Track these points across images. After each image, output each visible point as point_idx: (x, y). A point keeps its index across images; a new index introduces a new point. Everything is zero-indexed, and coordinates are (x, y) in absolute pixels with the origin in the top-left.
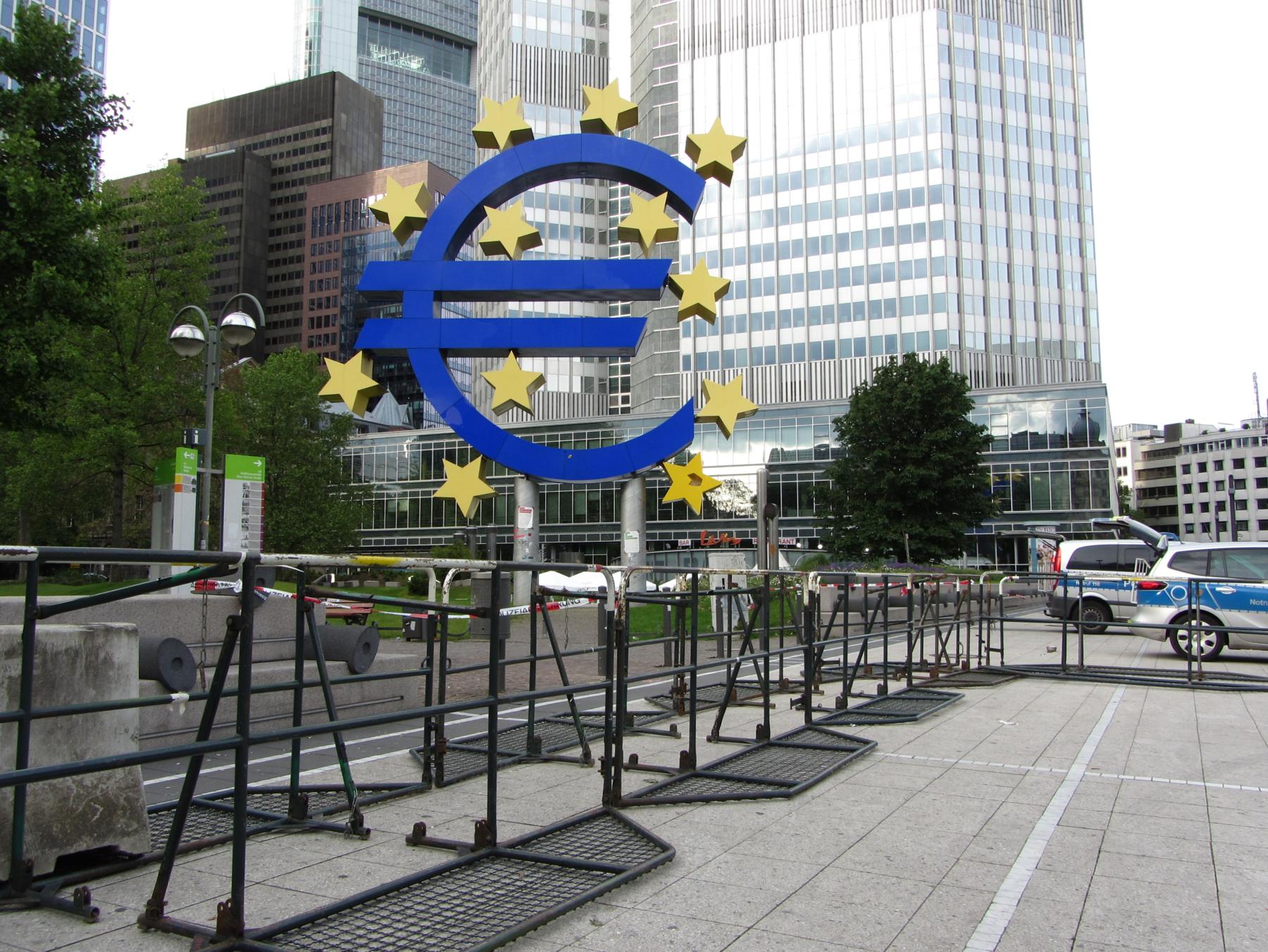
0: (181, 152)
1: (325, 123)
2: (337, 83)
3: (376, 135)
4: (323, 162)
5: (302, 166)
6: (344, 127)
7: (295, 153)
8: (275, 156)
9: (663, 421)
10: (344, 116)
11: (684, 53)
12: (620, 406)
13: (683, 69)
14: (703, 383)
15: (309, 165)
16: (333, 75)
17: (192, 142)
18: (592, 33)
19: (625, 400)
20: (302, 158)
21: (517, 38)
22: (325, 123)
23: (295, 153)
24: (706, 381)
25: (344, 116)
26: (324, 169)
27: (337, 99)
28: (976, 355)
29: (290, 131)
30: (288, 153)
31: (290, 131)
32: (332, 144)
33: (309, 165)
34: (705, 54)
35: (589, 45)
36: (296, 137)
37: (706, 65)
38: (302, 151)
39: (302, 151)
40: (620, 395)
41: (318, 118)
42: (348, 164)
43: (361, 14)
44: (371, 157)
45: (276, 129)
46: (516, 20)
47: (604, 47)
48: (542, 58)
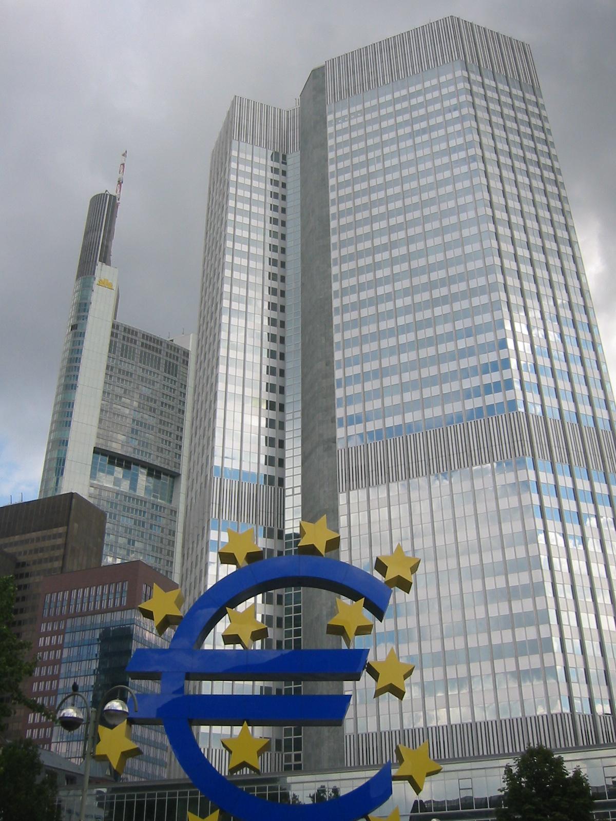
2: (74, 501)
3: (99, 540)
4: (57, 559)
5: (40, 561)
7: (36, 551)
8: (20, 553)
9: (367, 780)
10: (76, 525)
11: (342, 484)
12: (293, 762)
13: (342, 498)
14: (397, 747)
15: (46, 560)
16: (71, 495)
18: (272, 471)
19: (298, 757)
22: (61, 530)
23: (36, 551)
24: (401, 747)
25: (76, 525)
27: (73, 512)
28: (584, 716)
30: (31, 551)
32: (65, 545)
33: (46, 560)
34: (358, 487)
35: (270, 480)
36: (38, 539)
37: (358, 496)
38: (42, 550)
39: (42, 550)
40: (293, 753)
41: (57, 526)
45: (24, 533)
47: (281, 482)
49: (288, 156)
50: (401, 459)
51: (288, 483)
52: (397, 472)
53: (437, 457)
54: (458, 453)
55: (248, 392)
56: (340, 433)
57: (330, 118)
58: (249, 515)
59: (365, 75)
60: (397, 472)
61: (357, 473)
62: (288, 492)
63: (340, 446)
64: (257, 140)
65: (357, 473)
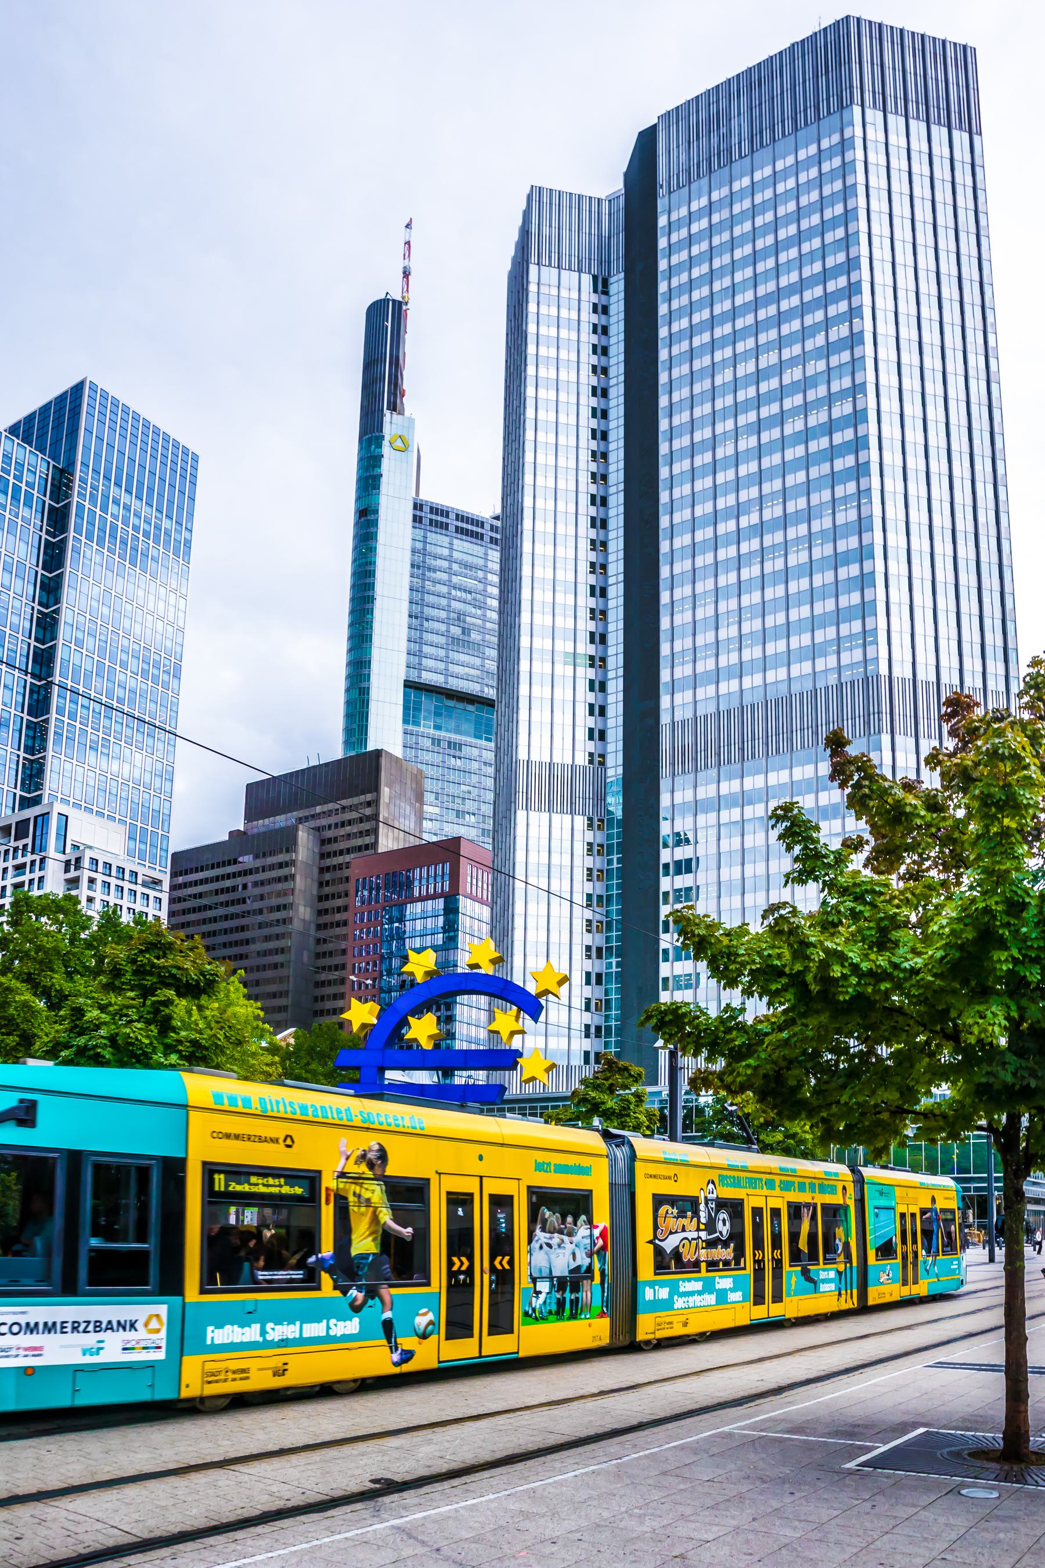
11: (665, 770)
13: (664, 784)
21: (522, 755)
48: (545, 773)
49: (612, 280)
50: (735, 736)
52: (729, 752)
53: (777, 735)
54: (802, 729)
55: (559, 645)
56: (665, 701)
57: (662, 221)
58: (562, 804)
59: (714, 140)
60: (729, 752)
61: (683, 754)
63: (665, 719)
64: (565, 263)
65: (683, 754)
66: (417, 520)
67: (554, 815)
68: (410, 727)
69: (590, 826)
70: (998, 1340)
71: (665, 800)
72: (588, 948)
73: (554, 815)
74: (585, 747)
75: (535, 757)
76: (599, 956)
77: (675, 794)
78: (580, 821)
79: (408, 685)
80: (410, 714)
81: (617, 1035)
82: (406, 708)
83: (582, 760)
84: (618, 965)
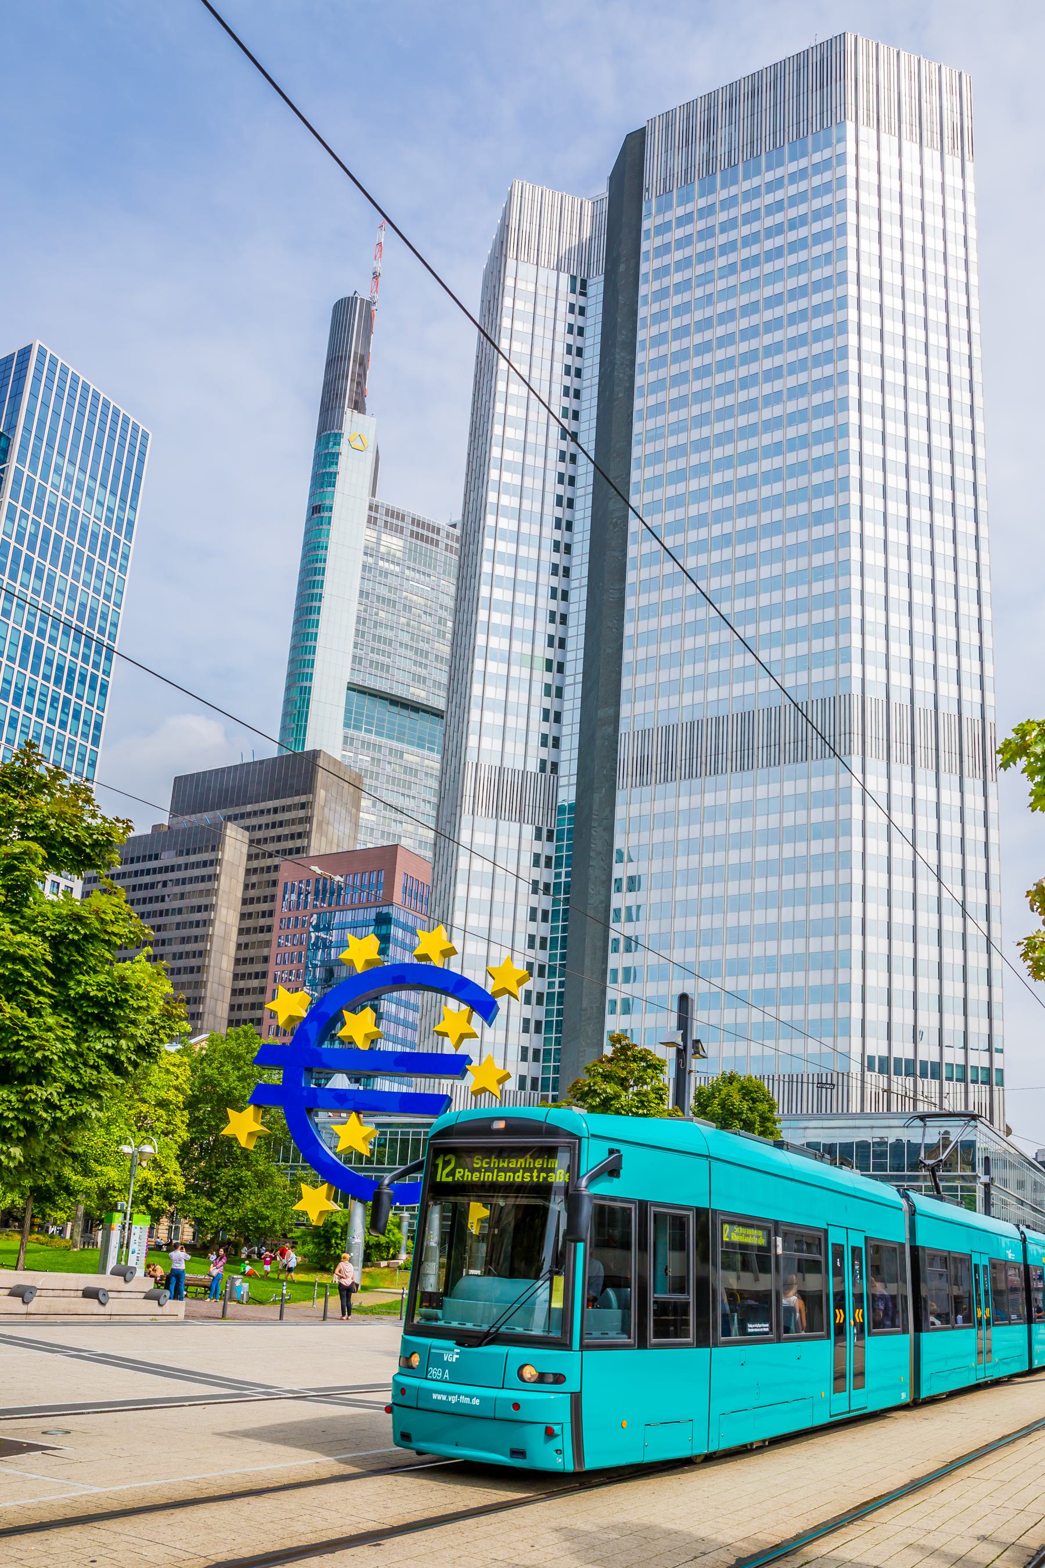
0: (165, 819)
1: (303, 799)
4: (300, 835)
5: (279, 839)
6: (322, 803)
7: (274, 825)
13: (620, 795)
16: (315, 754)
17: (177, 808)
20: (279, 831)
21: (471, 757)
22: (303, 799)
23: (274, 825)
26: (298, 843)
29: (271, 804)
30: (267, 825)
31: (271, 804)
36: (276, 811)
38: (281, 824)
39: (281, 824)
42: (324, 839)
43: (349, 689)
44: (347, 831)
45: (257, 802)
46: (473, 741)
47: (555, 766)
51: (563, 770)
56: (625, 710)
62: (563, 781)
66: (372, 521)
67: (501, 822)
68: (351, 732)
69: (538, 837)
70: (960, 1108)
71: (620, 812)
72: (535, 883)
73: (501, 822)
74: (537, 753)
75: (485, 761)
76: (548, 865)
77: (631, 805)
78: (529, 830)
79: (352, 688)
80: (351, 720)
81: (563, 948)
82: (348, 711)
83: (533, 767)
84: (567, 875)
